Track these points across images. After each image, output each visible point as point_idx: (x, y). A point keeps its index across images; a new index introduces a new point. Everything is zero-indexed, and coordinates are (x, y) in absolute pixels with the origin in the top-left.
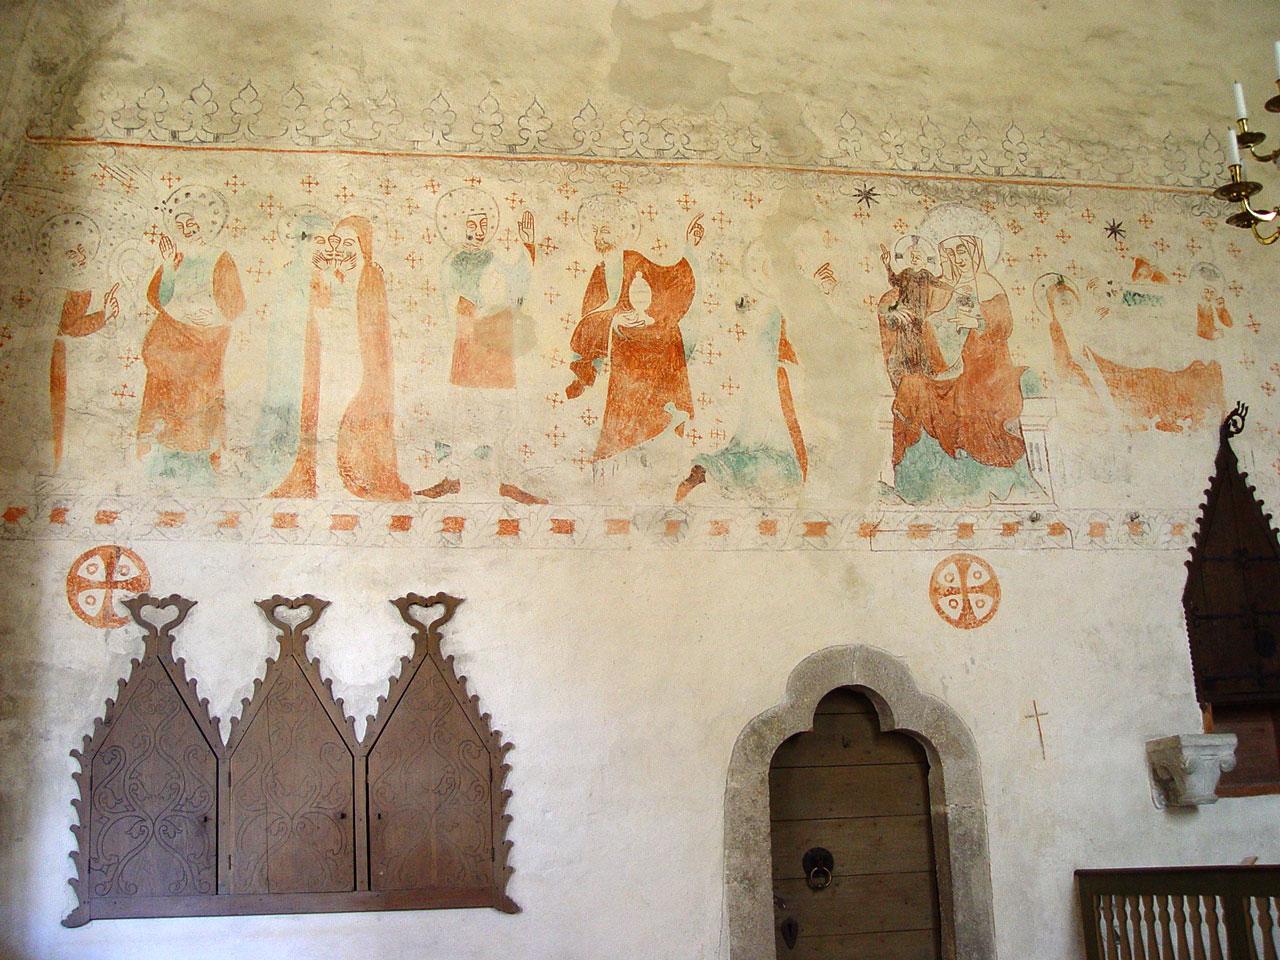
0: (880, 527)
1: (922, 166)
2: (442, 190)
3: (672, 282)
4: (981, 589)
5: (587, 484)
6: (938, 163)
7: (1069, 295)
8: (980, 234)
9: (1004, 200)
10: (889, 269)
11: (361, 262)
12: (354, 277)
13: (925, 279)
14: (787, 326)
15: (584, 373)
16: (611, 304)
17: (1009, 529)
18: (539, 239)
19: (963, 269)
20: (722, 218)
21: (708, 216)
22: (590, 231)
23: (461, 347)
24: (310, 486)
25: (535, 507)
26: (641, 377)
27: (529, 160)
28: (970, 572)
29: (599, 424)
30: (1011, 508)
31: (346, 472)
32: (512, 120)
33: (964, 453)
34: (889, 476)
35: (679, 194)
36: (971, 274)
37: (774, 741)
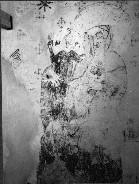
10: (51, 52)
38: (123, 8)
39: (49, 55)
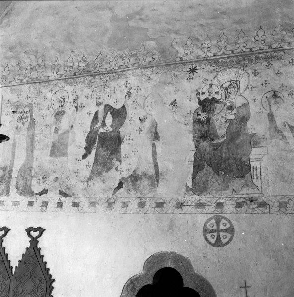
0: (185, 204)
1: (218, 54)
2: (53, 92)
3: (119, 114)
4: (226, 231)
5: (85, 189)
6: (225, 52)
7: (278, 100)
8: (239, 79)
9: (252, 62)
10: (199, 99)
11: (29, 119)
12: (27, 124)
13: (214, 101)
14: (158, 127)
15: (88, 150)
16: (99, 125)
17: (239, 205)
18: (79, 104)
19: (230, 95)
20: (138, 88)
21: (133, 88)
22: (95, 99)
23: (54, 144)
24: (8, 193)
25: (68, 198)
26: (106, 150)
27: (79, 77)
28: (221, 223)
29: (91, 168)
30: (241, 196)
31: (17, 187)
32: (77, 64)
33: (223, 173)
34: (190, 184)
35: (124, 82)
36: (233, 96)
37: (139, 287)
38: (245, 69)
39: (197, 101)
